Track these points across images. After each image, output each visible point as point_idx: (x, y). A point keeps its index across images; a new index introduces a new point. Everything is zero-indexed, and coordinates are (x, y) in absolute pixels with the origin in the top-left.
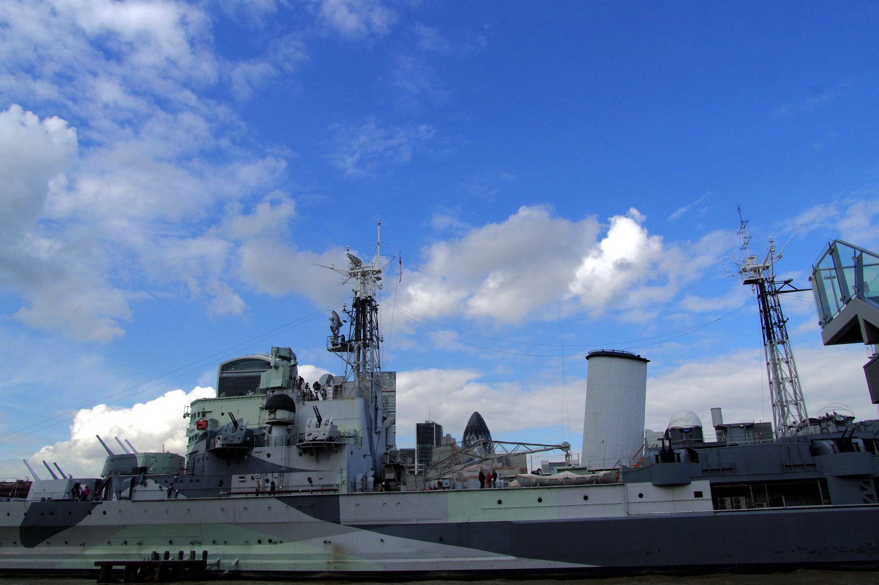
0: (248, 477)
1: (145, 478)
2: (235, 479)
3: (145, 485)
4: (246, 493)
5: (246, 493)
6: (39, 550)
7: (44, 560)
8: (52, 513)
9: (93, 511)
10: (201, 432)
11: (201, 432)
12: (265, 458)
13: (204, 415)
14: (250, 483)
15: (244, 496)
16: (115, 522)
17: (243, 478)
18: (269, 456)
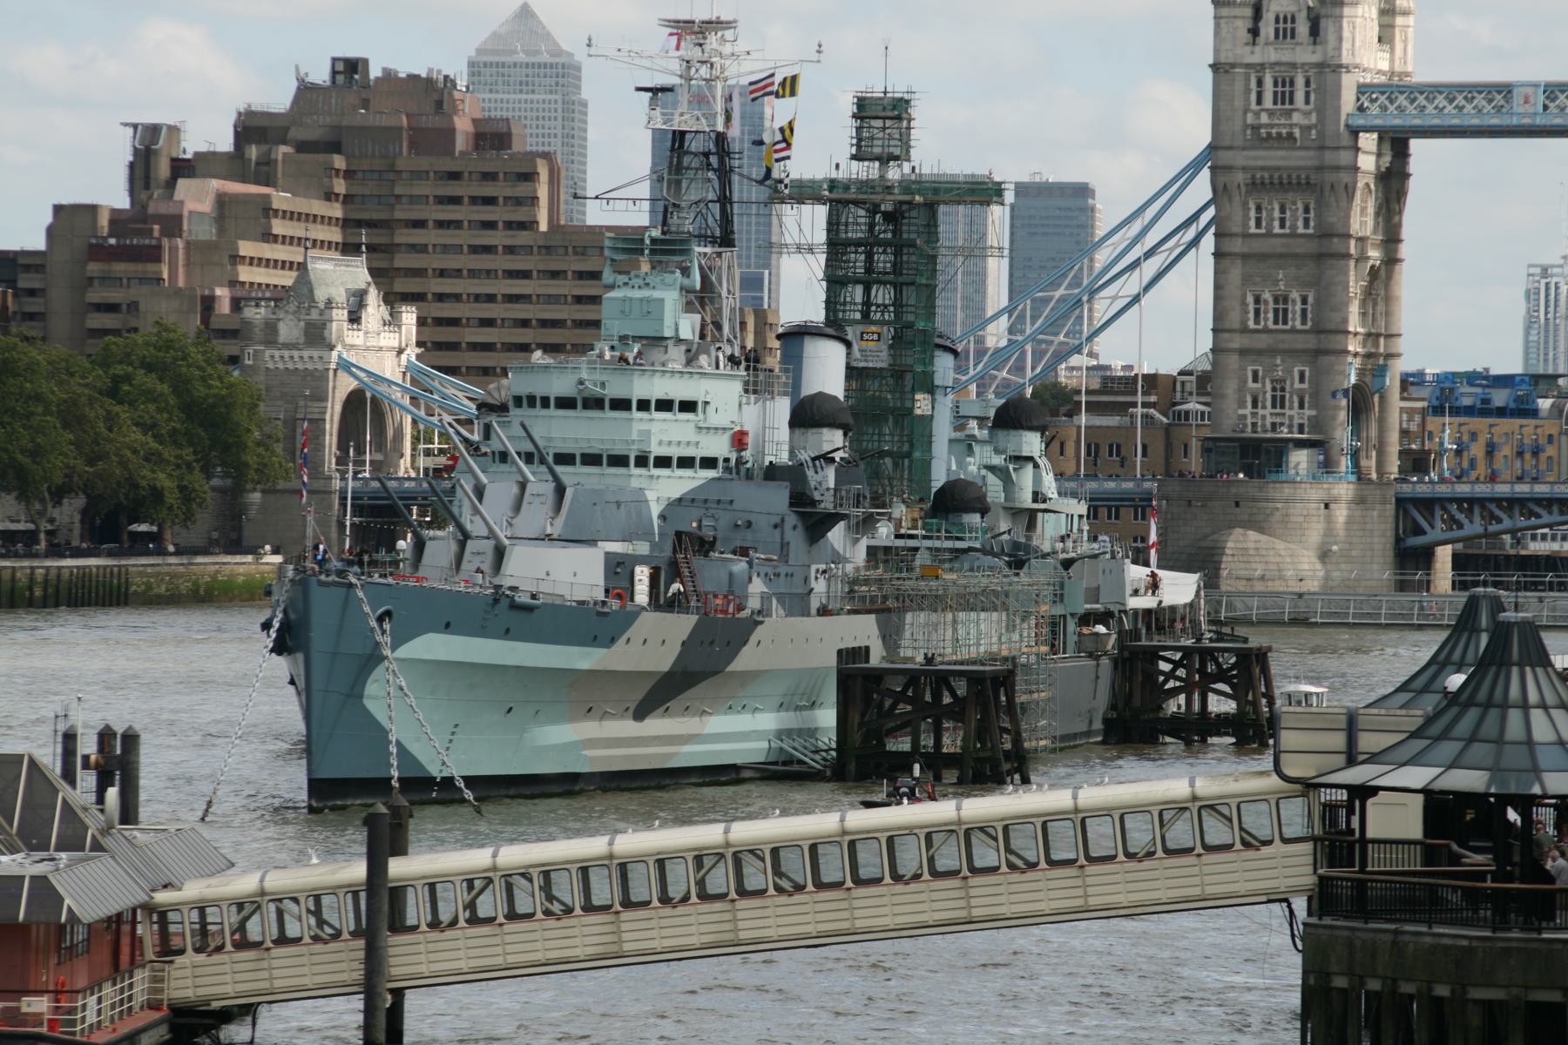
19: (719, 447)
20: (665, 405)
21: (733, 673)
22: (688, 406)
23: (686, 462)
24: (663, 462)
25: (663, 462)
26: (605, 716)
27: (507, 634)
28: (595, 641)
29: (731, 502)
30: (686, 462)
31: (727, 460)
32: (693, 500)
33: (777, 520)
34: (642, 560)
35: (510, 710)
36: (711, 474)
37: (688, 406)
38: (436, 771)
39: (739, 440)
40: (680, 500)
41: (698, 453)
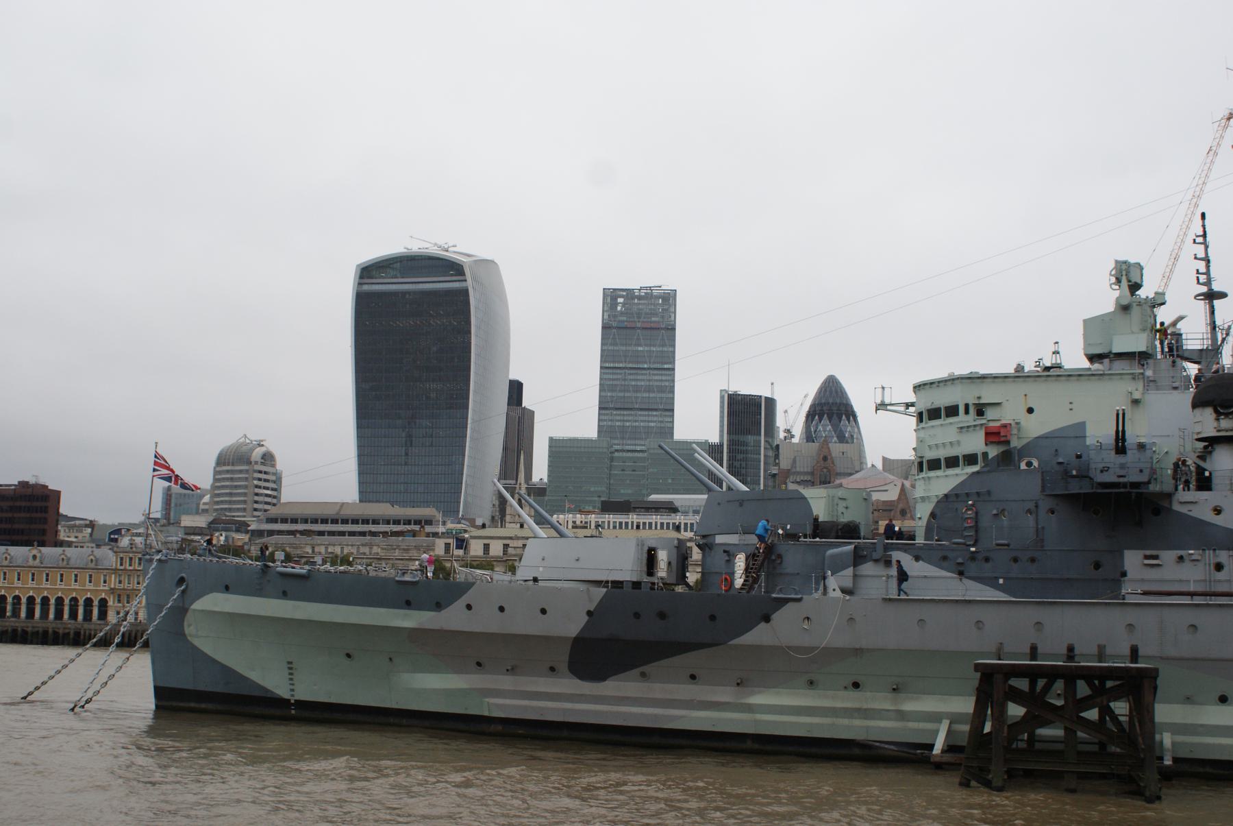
0: (1168, 556)
1: (887, 548)
2: (1132, 560)
4: (1192, 594)
5: (1192, 594)
6: (611, 687)
7: (550, 704)
8: (662, 615)
9: (776, 617)
10: (993, 452)
11: (993, 452)
12: (1210, 517)
13: (980, 413)
14: (1180, 570)
15: (1186, 600)
16: (842, 641)
17: (1156, 557)
18: (1218, 511)
19: (975, 443)
21: (757, 650)
22: (952, 411)
23: (952, 462)
24: (934, 465)
25: (934, 465)
26: (512, 670)
27: (284, 595)
28: (408, 604)
29: (989, 493)
30: (952, 462)
31: (985, 455)
32: (957, 496)
33: (1031, 506)
34: (739, 548)
35: (348, 656)
36: (975, 468)
37: (952, 411)
38: (283, 692)
39: (993, 436)
41: (959, 451)
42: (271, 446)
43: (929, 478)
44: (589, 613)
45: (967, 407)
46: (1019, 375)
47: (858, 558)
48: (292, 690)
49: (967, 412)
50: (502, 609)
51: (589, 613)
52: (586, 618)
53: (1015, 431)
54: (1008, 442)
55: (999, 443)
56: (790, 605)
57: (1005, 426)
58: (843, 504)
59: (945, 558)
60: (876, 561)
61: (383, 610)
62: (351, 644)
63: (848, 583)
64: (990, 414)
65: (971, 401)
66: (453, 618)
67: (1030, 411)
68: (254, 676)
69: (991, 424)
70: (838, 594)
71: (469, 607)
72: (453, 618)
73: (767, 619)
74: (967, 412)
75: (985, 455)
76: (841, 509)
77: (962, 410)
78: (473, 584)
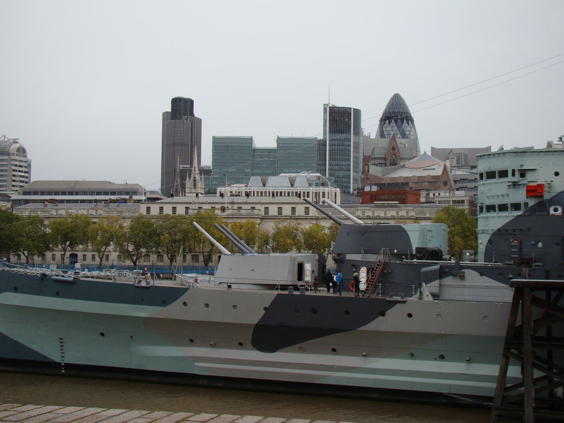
3: (462, 277)
9: (389, 313)
10: (532, 202)
11: (532, 202)
16: (432, 329)
19: (520, 196)
20: (491, 175)
21: (377, 334)
23: (503, 208)
24: (491, 208)
25: (491, 208)
26: (214, 346)
27: (57, 294)
29: (529, 229)
30: (503, 208)
31: (526, 204)
32: (507, 230)
34: (363, 263)
35: (102, 334)
37: (503, 174)
40: (499, 230)
42: (23, 143)
43: (487, 217)
44: (265, 309)
45: (513, 171)
46: (549, 151)
47: (443, 273)
48: (63, 357)
49: (513, 174)
50: (207, 305)
51: (265, 309)
52: (264, 312)
53: (546, 189)
54: (542, 196)
55: (536, 197)
56: (398, 305)
57: (541, 186)
58: (430, 234)
59: (500, 274)
60: (454, 275)
61: (126, 305)
62: (104, 326)
63: (436, 291)
64: (530, 177)
65: (517, 168)
66: (174, 311)
67: (557, 174)
68: (35, 347)
69: (531, 184)
70: (430, 298)
71: (185, 304)
72: (174, 311)
73: (383, 314)
74: (513, 174)
75: (526, 204)
76: (428, 238)
77: (510, 173)
78: (186, 290)
